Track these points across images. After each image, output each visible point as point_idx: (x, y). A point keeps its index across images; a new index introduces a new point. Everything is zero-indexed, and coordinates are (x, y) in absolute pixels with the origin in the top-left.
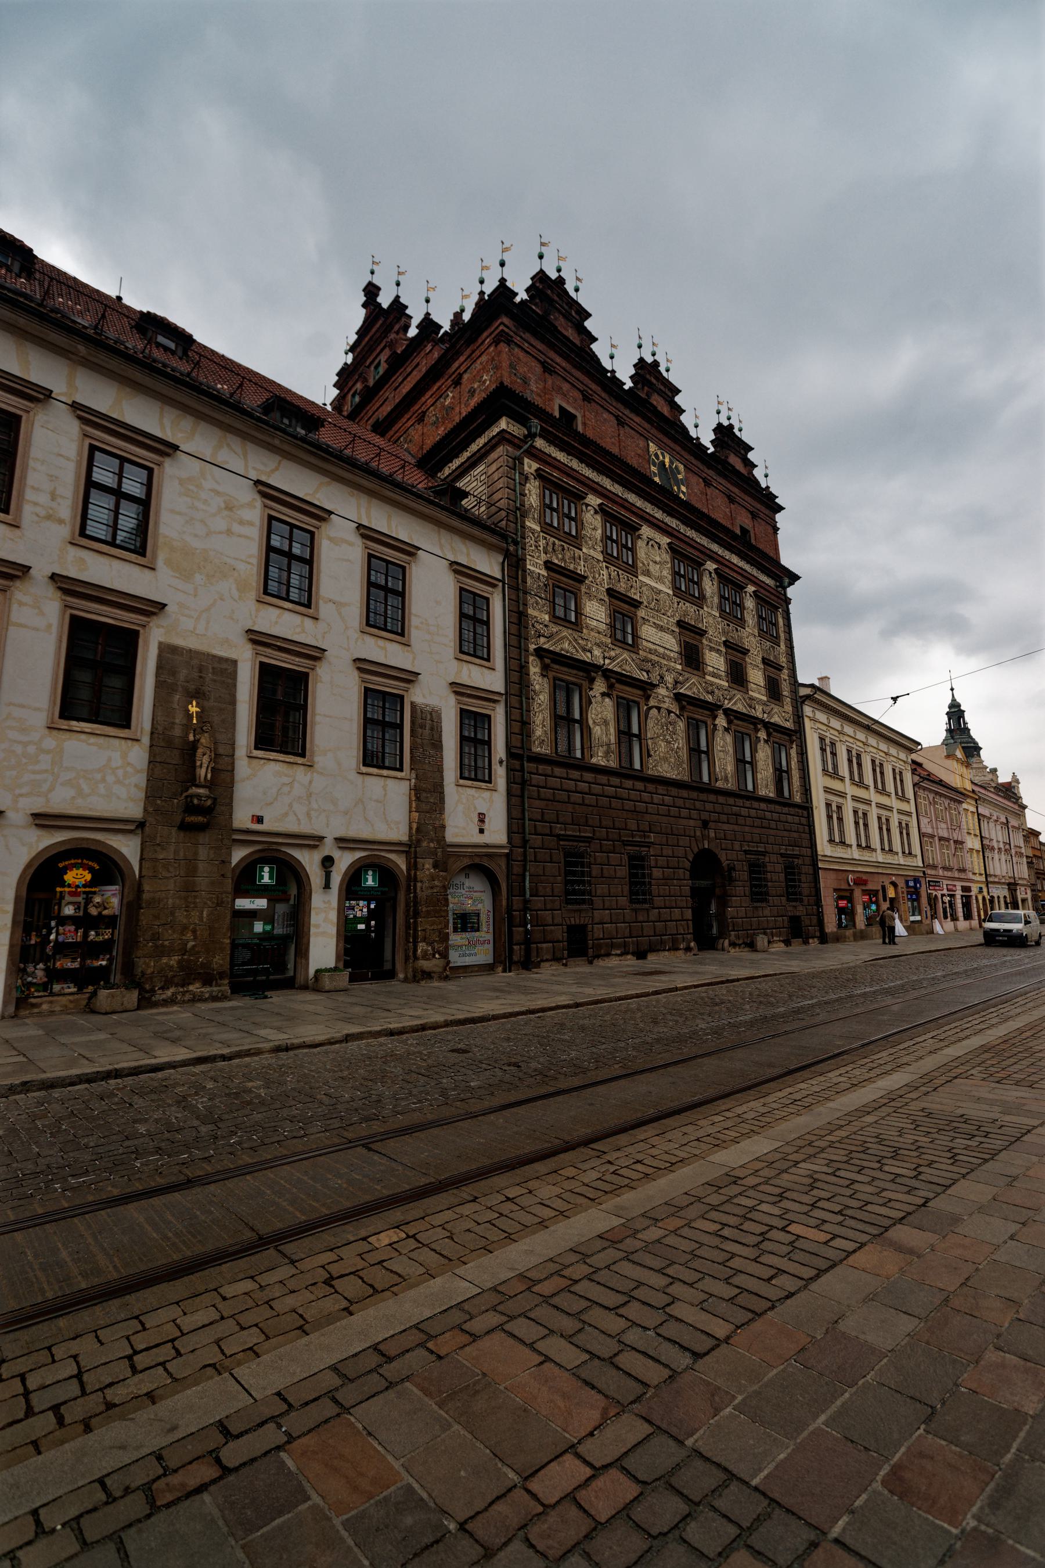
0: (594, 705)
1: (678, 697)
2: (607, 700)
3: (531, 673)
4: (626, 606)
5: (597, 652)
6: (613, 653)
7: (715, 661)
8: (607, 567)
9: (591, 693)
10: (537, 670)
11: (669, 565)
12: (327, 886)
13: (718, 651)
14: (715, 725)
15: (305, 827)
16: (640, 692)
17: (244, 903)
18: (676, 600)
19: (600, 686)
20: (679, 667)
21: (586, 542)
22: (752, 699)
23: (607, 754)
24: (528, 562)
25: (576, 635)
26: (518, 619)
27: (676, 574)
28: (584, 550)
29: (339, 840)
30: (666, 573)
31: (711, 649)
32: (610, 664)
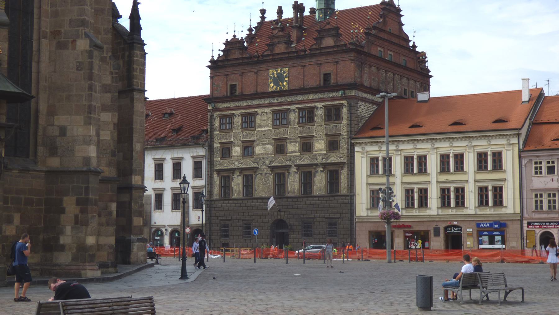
1: (269, 167)
2: (239, 177)
3: (214, 176)
4: (249, 143)
5: (236, 163)
6: (243, 161)
7: (293, 147)
9: (233, 177)
10: (216, 175)
11: (272, 118)
12: (166, 234)
13: (296, 142)
14: (289, 173)
15: (163, 224)
16: (252, 171)
17: (156, 238)
18: (274, 130)
19: (237, 173)
21: (235, 128)
22: (316, 155)
23: (238, 194)
24: (214, 145)
25: (229, 160)
26: (211, 163)
27: (274, 120)
28: (234, 131)
29: (168, 226)
30: (270, 122)
31: (291, 142)
32: (241, 166)
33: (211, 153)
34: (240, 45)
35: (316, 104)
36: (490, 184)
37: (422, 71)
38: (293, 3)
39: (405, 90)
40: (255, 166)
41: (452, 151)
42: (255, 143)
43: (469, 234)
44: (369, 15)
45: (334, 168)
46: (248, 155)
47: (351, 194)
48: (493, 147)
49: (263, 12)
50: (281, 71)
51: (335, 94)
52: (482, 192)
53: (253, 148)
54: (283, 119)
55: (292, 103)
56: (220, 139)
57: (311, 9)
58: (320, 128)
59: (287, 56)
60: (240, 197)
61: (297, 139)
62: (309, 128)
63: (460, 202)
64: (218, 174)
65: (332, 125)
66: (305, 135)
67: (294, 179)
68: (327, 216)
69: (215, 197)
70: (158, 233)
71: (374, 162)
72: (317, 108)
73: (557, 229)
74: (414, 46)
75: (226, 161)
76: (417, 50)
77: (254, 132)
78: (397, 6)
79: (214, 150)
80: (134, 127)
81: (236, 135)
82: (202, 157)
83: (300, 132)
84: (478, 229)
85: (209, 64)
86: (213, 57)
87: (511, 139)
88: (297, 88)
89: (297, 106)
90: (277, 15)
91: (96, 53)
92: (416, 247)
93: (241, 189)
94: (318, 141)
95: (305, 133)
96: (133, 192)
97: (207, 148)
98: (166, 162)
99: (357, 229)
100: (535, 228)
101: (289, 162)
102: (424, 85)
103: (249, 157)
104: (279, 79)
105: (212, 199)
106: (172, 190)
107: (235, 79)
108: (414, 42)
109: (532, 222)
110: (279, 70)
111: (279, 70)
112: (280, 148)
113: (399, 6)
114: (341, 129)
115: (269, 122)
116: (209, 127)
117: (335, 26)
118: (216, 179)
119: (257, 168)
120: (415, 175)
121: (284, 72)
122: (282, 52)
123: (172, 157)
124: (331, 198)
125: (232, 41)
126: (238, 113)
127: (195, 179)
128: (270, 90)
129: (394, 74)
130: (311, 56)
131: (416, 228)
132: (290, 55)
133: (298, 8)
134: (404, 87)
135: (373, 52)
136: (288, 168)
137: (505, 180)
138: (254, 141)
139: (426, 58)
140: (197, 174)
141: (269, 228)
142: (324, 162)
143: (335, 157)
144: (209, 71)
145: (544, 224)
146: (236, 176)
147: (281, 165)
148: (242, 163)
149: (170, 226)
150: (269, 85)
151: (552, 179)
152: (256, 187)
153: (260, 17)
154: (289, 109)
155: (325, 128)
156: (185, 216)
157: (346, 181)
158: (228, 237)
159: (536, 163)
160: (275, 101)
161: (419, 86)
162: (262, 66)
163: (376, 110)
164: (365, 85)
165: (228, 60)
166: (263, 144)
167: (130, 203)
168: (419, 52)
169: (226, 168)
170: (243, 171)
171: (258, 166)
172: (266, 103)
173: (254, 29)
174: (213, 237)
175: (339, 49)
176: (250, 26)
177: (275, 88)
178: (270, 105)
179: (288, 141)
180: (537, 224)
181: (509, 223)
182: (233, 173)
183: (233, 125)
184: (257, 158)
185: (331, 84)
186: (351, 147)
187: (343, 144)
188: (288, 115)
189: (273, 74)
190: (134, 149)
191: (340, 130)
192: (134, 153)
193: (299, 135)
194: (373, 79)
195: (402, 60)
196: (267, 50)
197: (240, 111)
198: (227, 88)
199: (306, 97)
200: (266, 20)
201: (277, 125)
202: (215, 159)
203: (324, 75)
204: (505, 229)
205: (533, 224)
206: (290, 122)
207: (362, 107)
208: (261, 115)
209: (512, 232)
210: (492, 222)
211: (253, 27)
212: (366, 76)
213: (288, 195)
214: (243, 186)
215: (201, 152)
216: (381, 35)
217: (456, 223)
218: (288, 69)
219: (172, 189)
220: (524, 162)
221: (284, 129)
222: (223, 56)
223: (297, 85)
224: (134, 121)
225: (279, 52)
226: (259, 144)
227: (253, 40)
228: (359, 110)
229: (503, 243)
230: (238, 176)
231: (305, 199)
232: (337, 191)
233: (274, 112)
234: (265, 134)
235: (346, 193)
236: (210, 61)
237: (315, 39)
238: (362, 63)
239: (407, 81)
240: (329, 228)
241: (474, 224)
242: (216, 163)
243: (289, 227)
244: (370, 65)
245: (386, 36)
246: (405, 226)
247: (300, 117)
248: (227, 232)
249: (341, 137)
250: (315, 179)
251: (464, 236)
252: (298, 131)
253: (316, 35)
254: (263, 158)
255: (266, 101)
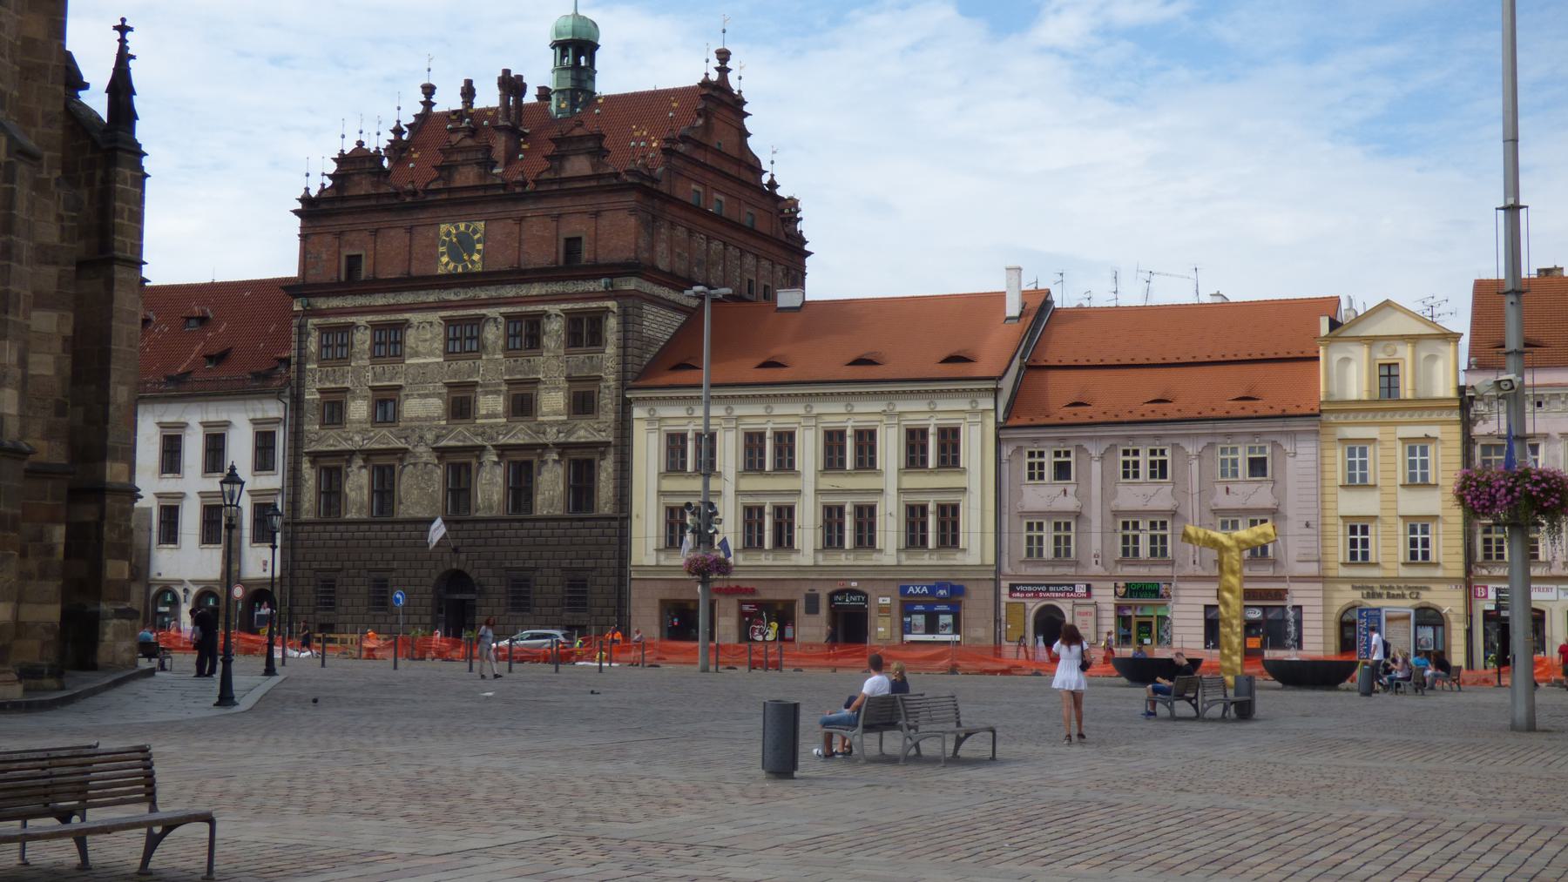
2: (364, 471)
5: (357, 438)
6: (372, 434)
7: (491, 405)
9: (349, 469)
10: (308, 465)
11: (442, 336)
13: (497, 393)
14: (481, 464)
15: (177, 577)
18: (446, 364)
19: (359, 462)
22: (543, 423)
23: (359, 510)
25: (339, 431)
26: (296, 436)
27: (447, 339)
29: (190, 581)
30: (439, 345)
31: (487, 393)
33: (297, 414)
34: (372, 165)
35: (546, 308)
36: (932, 500)
37: (789, 242)
38: (500, 75)
39: (750, 281)
40: (400, 445)
41: (850, 424)
42: (402, 393)
43: (884, 610)
44: (673, 109)
45: (586, 455)
46: (385, 421)
47: (624, 515)
48: (940, 416)
49: (429, 90)
50: (467, 227)
51: (591, 286)
52: (915, 516)
53: (397, 404)
54: (467, 338)
55: (491, 301)
56: (319, 381)
57: (540, 88)
58: (554, 362)
59: (481, 193)
60: (364, 516)
61: (499, 385)
62: (529, 361)
63: (866, 537)
64: (313, 463)
65: (581, 356)
66: (519, 377)
67: (491, 479)
68: (565, 563)
69: (304, 517)
70: (165, 597)
71: (675, 443)
72: (549, 317)
73: (1071, 601)
74: (773, 184)
75: (331, 433)
76: (780, 192)
77: (401, 368)
78: (736, 92)
79: (306, 406)
80: (113, 347)
81: (357, 372)
82: (276, 421)
83: (509, 371)
84: (903, 599)
85: (299, 206)
86: (307, 189)
87: (979, 400)
88: (503, 268)
89: (503, 310)
90: (461, 99)
91: (22, 169)
92: (764, 637)
93: (366, 498)
95: (520, 372)
96: (108, 501)
97: (288, 401)
98: (188, 431)
99: (634, 594)
100: (1025, 597)
101: (480, 439)
102: (793, 272)
103: (388, 424)
104: (463, 245)
105: (297, 520)
106: (202, 497)
107: (357, 243)
108: (772, 175)
109: (1019, 585)
110: (462, 227)
111: (462, 227)
112: (461, 406)
113: (740, 92)
114: (601, 366)
115: (436, 345)
116: (294, 353)
117: (595, 130)
118: (309, 473)
119: (405, 451)
120: (768, 475)
121: (475, 232)
122: (471, 184)
123: (205, 420)
124: (575, 524)
125: (355, 154)
126: (363, 323)
127: (258, 473)
128: (441, 271)
129: (725, 244)
130: (538, 196)
131: (767, 594)
132: (489, 193)
133: (511, 85)
134: (747, 276)
135: (680, 193)
136: (477, 453)
137: (964, 490)
138: (400, 387)
139: (798, 211)
140: (264, 459)
141: (430, 589)
142: (563, 440)
143: (586, 430)
144: (297, 221)
145: (1044, 588)
146: (354, 467)
147: (460, 444)
148: (370, 439)
149: (194, 582)
150: (437, 259)
151: (1065, 491)
152: (402, 494)
153: (422, 103)
154: (484, 315)
155: (565, 365)
156: (231, 558)
157: (611, 486)
158: (333, 609)
159: (1031, 454)
160: (450, 296)
161: (781, 274)
162: (424, 216)
163: (682, 325)
164: (661, 267)
165: (343, 199)
166: (420, 396)
167: (99, 526)
168: (782, 199)
169: (332, 448)
170: (373, 458)
171: (406, 446)
172: (431, 300)
173: (406, 129)
174: (297, 609)
175: (603, 182)
176: (398, 122)
177: (451, 266)
178: (440, 305)
179: (479, 390)
180: (1030, 588)
181: (970, 587)
182: (349, 462)
183: (352, 348)
184: (406, 429)
185: (583, 262)
186: (625, 408)
187: (607, 401)
188: (481, 330)
189: (448, 234)
190: (112, 400)
191: (600, 369)
192: (112, 409)
193: (506, 377)
194: (679, 254)
195: (744, 215)
196: (436, 180)
197: (369, 318)
198: (339, 262)
199: (524, 290)
200: (435, 109)
201: (454, 352)
202: (306, 427)
203: (568, 240)
204: (961, 599)
205: (1022, 588)
206: (484, 347)
207: (652, 317)
208: (418, 328)
209: (976, 606)
210: (933, 584)
211: (406, 126)
212: (662, 248)
213: (478, 515)
214: (372, 492)
215: (273, 409)
216: (700, 156)
217: (854, 584)
218: (482, 223)
219: (203, 495)
220: (1006, 451)
221: (471, 362)
222: (330, 187)
223: (502, 263)
224: (114, 334)
225: (466, 185)
226: (412, 395)
227: (404, 155)
228: (645, 323)
229: (956, 630)
230: (361, 467)
231: (517, 525)
232: (591, 507)
233: (448, 322)
235: (610, 512)
236: (301, 200)
237: (547, 157)
238: (654, 217)
239: (754, 262)
240: (569, 592)
241: (894, 588)
242: (310, 436)
243: (477, 588)
244: (672, 223)
245: (709, 159)
246: (741, 589)
247: (509, 336)
248: (331, 598)
249: (602, 385)
250: (540, 478)
251: (873, 613)
252: (503, 368)
253: (550, 149)
254: (421, 428)
255: (432, 297)
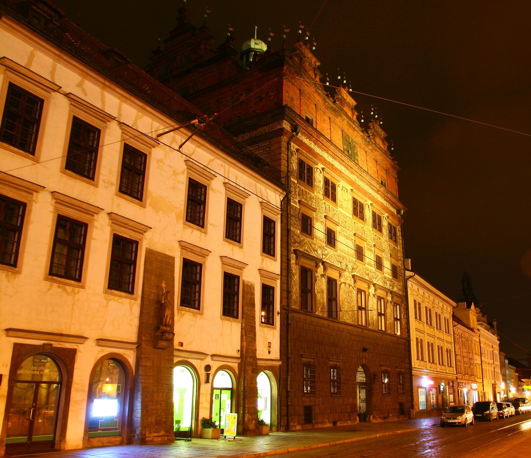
0: (318, 282)
2: (323, 279)
8: (325, 203)
13: (371, 250)
14: (369, 293)
20: (354, 260)
24: (291, 200)
28: (315, 194)
94: (386, 261)
152: (341, 303)
234: (346, 221)
